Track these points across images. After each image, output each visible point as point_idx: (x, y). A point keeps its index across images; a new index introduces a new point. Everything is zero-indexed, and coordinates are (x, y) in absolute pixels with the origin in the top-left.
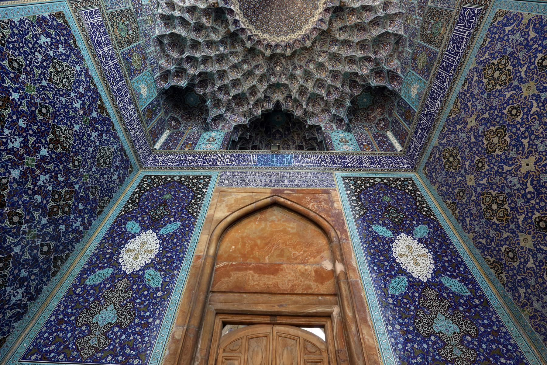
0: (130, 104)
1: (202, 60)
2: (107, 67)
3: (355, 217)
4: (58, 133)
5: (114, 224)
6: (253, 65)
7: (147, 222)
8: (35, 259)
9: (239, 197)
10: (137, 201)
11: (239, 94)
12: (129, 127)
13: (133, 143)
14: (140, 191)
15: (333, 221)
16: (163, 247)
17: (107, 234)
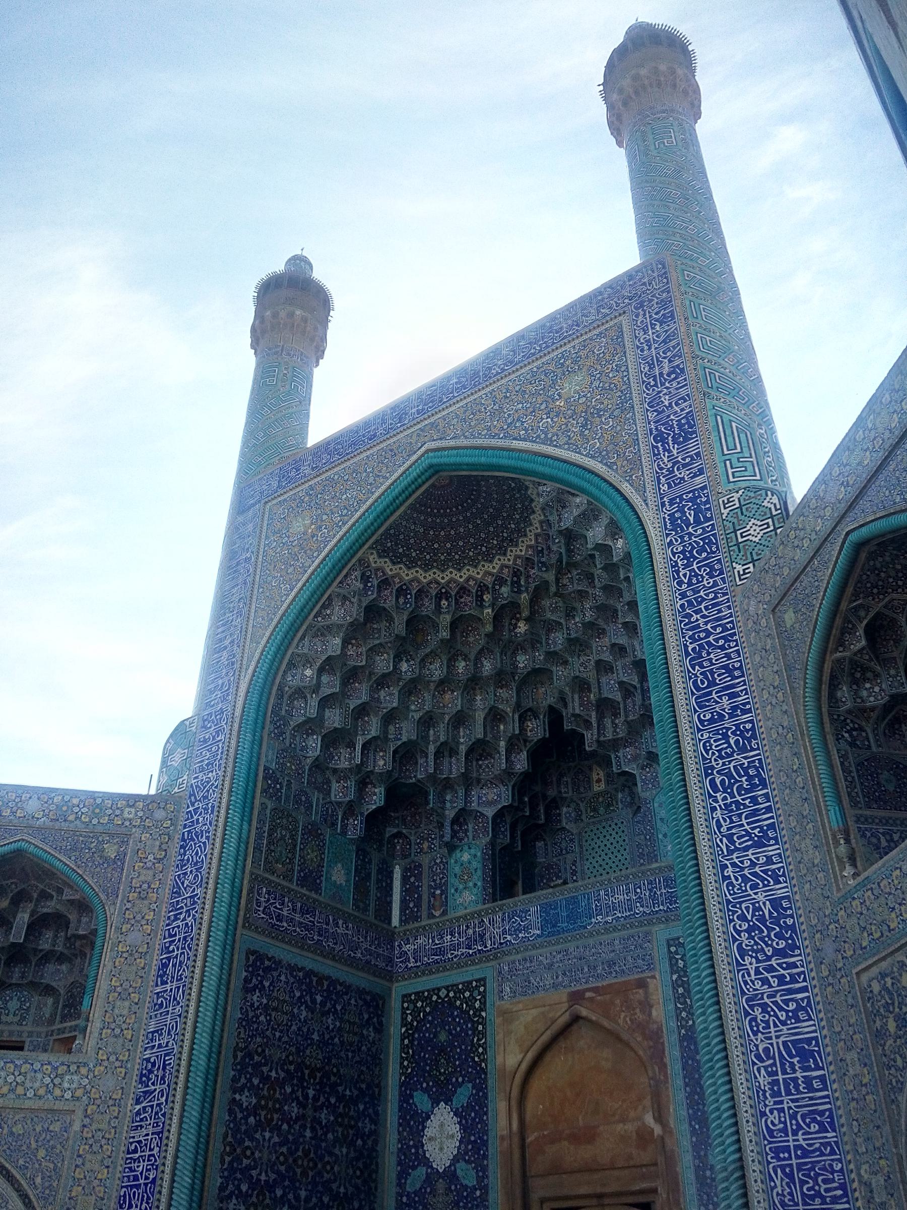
0: (337, 925)
1: (385, 721)
2: (298, 930)
3: (680, 1034)
4: (308, 1063)
5: (400, 1101)
6: (472, 657)
7: (434, 1089)
8: (356, 1187)
9: (530, 1018)
10: (411, 1051)
11: (474, 744)
12: (353, 955)
13: (367, 967)
14: (407, 1030)
15: (650, 1047)
16: (464, 1128)
17: (400, 1117)
